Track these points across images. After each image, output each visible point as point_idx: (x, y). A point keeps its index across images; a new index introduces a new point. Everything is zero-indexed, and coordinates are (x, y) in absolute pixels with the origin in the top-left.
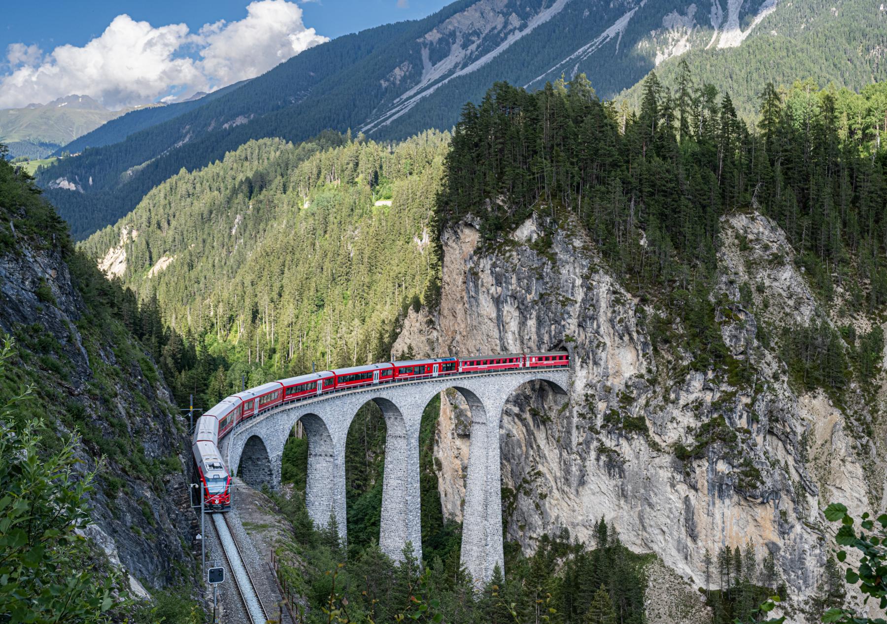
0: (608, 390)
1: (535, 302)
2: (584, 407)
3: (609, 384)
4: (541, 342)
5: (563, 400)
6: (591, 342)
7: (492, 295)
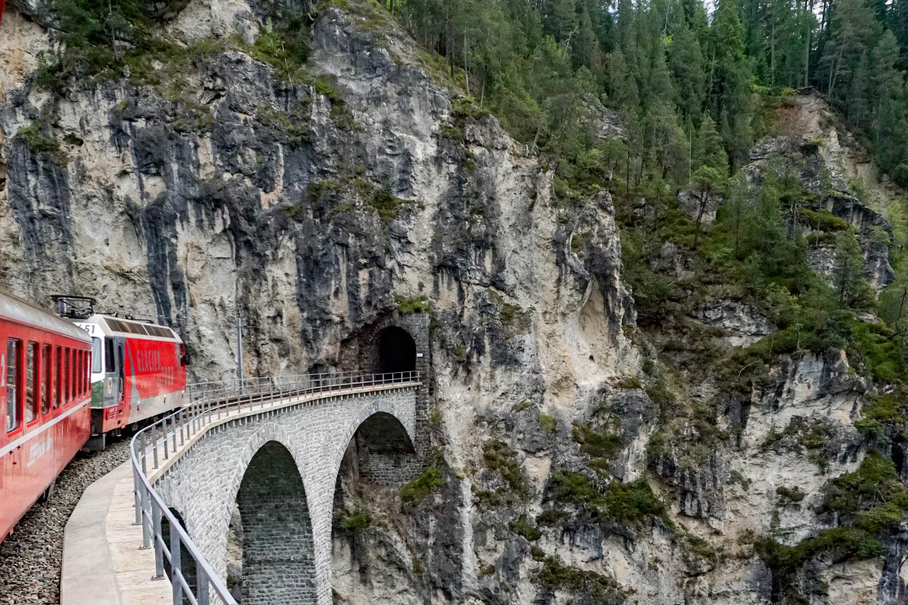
0: (553, 427)
1: (286, 217)
2: (486, 477)
3: (544, 410)
4: (319, 319)
5: (409, 467)
6: (484, 308)
7: (128, 199)
